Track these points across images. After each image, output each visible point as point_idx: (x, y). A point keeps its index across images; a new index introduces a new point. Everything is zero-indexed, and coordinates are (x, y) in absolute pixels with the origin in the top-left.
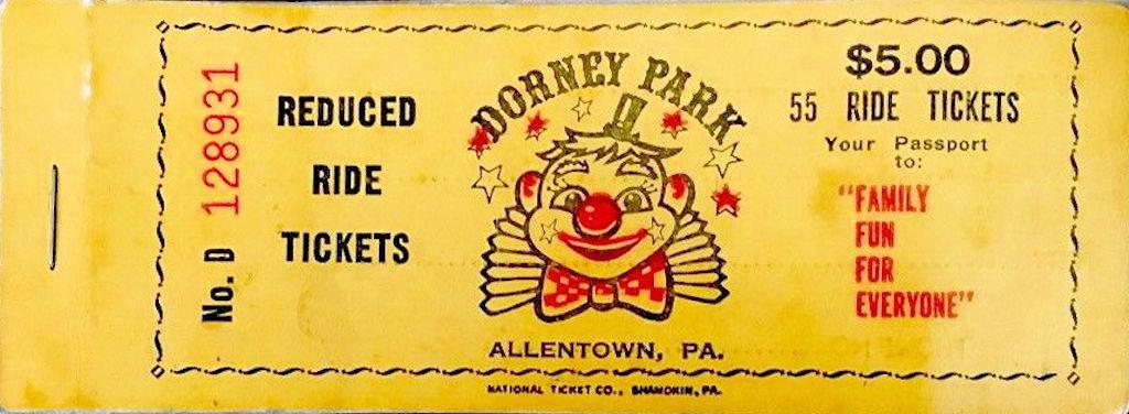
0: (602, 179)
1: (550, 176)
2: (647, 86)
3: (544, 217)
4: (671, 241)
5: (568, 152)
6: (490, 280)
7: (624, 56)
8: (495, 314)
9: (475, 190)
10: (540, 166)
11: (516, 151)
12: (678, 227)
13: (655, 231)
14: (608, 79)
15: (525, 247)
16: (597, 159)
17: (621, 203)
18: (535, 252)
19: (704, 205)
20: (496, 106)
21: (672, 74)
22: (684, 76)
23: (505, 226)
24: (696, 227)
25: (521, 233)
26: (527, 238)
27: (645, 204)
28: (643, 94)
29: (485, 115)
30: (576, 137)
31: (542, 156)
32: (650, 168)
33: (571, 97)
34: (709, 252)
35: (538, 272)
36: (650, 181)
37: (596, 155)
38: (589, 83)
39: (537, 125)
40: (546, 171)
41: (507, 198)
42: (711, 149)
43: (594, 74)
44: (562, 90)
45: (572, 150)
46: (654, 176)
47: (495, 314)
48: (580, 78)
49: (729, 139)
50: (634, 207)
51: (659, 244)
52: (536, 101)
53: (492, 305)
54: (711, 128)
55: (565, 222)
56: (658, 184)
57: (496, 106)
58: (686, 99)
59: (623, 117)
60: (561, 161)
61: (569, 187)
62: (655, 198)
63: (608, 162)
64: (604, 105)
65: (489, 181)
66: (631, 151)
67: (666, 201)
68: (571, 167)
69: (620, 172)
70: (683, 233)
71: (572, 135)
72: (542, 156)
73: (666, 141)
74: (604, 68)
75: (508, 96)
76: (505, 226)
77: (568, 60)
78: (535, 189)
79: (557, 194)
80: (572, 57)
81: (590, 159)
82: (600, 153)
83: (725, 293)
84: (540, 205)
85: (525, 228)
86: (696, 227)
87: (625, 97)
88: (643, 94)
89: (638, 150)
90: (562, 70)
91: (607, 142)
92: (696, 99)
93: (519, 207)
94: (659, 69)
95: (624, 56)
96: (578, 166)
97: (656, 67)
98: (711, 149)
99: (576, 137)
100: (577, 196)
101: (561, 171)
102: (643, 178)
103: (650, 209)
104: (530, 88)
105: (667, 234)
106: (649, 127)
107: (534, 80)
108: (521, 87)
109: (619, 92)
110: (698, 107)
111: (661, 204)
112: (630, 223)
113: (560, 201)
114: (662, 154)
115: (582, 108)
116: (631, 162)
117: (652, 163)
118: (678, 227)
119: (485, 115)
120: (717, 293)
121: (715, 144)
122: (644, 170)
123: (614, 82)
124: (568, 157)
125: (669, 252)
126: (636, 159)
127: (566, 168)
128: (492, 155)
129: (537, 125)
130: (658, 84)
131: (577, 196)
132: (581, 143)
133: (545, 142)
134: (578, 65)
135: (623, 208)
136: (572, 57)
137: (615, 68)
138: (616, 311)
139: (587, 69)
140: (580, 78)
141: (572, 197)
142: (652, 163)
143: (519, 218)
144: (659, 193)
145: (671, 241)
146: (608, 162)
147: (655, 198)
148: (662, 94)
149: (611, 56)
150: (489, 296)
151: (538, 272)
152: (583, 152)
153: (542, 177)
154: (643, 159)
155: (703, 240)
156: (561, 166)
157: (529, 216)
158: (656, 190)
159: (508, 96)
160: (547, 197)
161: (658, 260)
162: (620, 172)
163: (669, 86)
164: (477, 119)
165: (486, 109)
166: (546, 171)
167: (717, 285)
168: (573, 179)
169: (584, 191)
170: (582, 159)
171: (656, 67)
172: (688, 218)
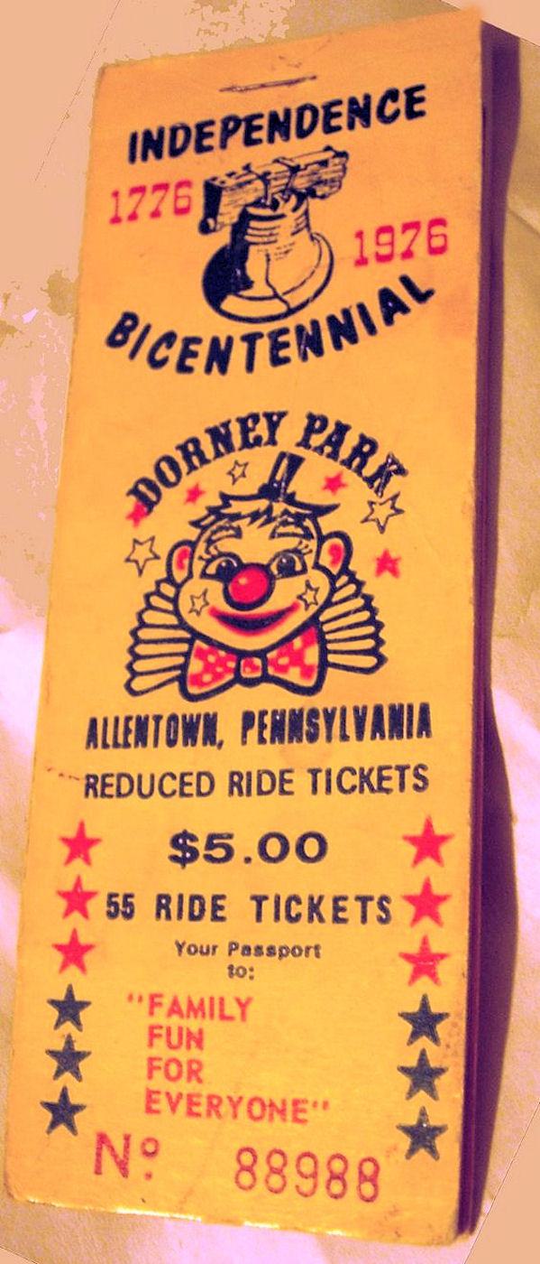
0: (256, 545)
1: (201, 549)
2: (305, 443)
3: (195, 586)
4: (328, 603)
5: (220, 517)
6: (137, 657)
7: (282, 415)
8: (142, 693)
9: (129, 564)
10: (193, 534)
11: (174, 519)
12: (333, 590)
13: (309, 597)
14: (265, 437)
15: (173, 620)
16: (252, 522)
17: (274, 569)
18: (182, 625)
19: (362, 565)
20: (153, 477)
21: (331, 428)
22: (342, 429)
23: (155, 600)
24: (352, 588)
25: (170, 607)
26: (176, 612)
27: (298, 567)
28: (301, 452)
29: (142, 488)
30: (231, 502)
31: (195, 524)
32: (306, 529)
33: (227, 461)
34: (365, 615)
35: (184, 647)
36: (305, 542)
37: (248, 520)
38: (246, 444)
39: (194, 494)
40: (199, 538)
41: (157, 570)
42: (371, 503)
43: (251, 436)
44: (218, 454)
45: (224, 516)
46: (308, 535)
47: (142, 693)
48: (237, 440)
49: (390, 490)
50: (288, 571)
51: (313, 609)
52: (192, 468)
53: (138, 684)
54: (370, 481)
55: (216, 588)
56: (313, 544)
57: (153, 477)
58: (345, 452)
59: (278, 477)
60: (214, 527)
61: (221, 555)
62: (310, 560)
63: (262, 525)
64: (259, 465)
65: (142, 553)
66: (286, 512)
67: (321, 562)
68: (224, 533)
69: (272, 536)
70: (336, 597)
71: (226, 499)
72: (195, 524)
73: (325, 499)
74: (262, 429)
75: (164, 466)
76: (155, 600)
77: (226, 425)
78: (186, 562)
79: (209, 562)
80: (229, 422)
81: (243, 523)
82: (255, 516)
83: (381, 660)
84: (190, 575)
85: (175, 601)
86: (352, 588)
87: (282, 455)
88: (301, 452)
89: (293, 510)
90: (220, 436)
91: (262, 504)
92: (357, 451)
93: (170, 579)
94: (318, 425)
95: (282, 415)
96: (231, 532)
97: (315, 423)
98: (371, 503)
99: (231, 502)
100: (229, 563)
101: (214, 538)
102: (297, 540)
103: (304, 570)
104: (187, 457)
105: (322, 598)
106: (307, 486)
107: (191, 452)
108: (178, 456)
109: (273, 452)
110: (357, 461)
111: (317, 566)
112: (284, 592)
113: (212, 569)
114: (319, 511)
115: (238, 471)
116: (285, 523)
117: (308, 523)
118: (333, 590)
119: (142, 488)
120: (370, 661)
121: (374, 498)
122: (299, 531)
123: (272, 441)
124: (221, 523)
125: (322, 619)
126: (290, 520)
127: (219, 535)
128: (149, 525)
129: (194, 494)
130: (317, 440)
131: (229, 563)
132: (236, 507)
133: (198, 510)
134: (235, 429)
135: (275, 572)
136: (229, 422)
137: (273, 427)
138: (264, 686)
139: (245, 431)
140: (237, 440)
141: (224, 564)
142: (308, 523)
143: (168, 590)
144: (313, 555)
145: (328, 603)
146: (262, 525)
147: (310, 560)
148: (320, 449)
149: (268, 416)
150: (134, 674)
151: (184, 647)
152: (238, 516)
153: (193, 545)
154: (299, 520)
155: (359, 602)
156: (214, 533)
157: (178, 587)
158: (311, 551)
159: (164, 466)
160: (198, 566)
161: (313, 628)
162: (272, 536)
163: (328, 441)
164: (135, 491)
165: (145, 481)
166: (199, 538)
167: (373, 652)
168: (228, 545)
169: (238, 560)
170: (235, 524)
171: (315, 423)
172: (344, 579)
